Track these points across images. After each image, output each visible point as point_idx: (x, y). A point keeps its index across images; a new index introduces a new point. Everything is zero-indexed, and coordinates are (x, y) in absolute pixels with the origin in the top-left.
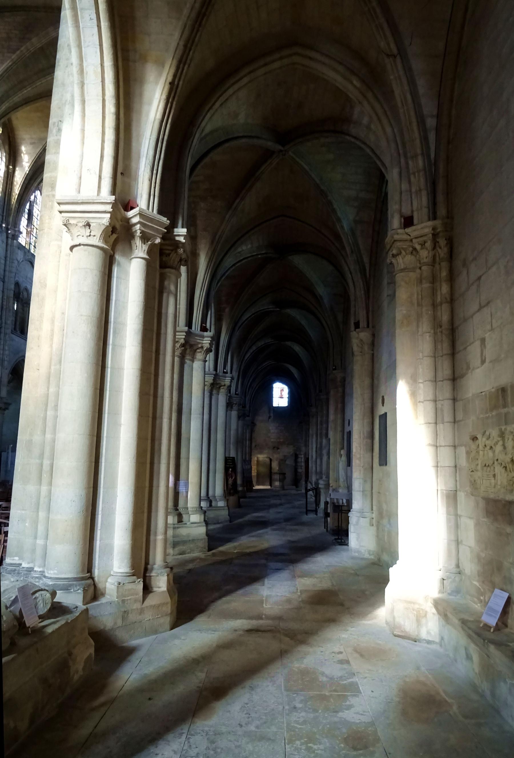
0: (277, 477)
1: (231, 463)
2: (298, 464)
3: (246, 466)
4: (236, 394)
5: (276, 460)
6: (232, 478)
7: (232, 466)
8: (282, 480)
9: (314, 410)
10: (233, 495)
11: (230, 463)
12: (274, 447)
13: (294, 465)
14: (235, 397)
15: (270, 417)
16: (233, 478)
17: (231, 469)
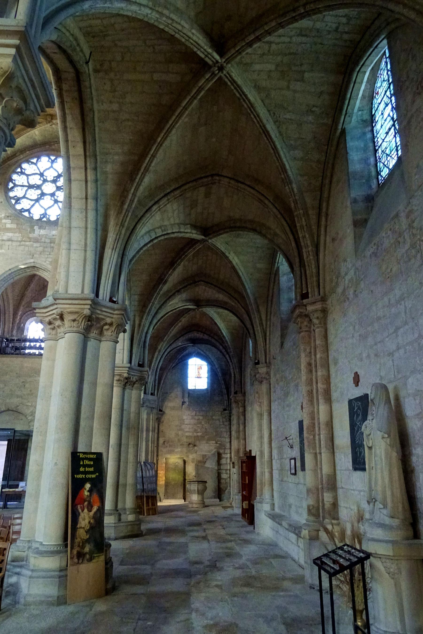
0: (194, 487)
1: (92, 469)
2: (222, 467)
3: (148, 472)
4: (111, 300)
5: (193, 462)
6: (90, 511)
7: (94, 476)
8: (201, 493)
9: (262, 370)
10: (90, 560)
11: (87, 469)
12: (189, 444)
13: (216, 468)
14: (108, 307)
15: (183, 403)
16: (95, 509)
17: (88, 486)
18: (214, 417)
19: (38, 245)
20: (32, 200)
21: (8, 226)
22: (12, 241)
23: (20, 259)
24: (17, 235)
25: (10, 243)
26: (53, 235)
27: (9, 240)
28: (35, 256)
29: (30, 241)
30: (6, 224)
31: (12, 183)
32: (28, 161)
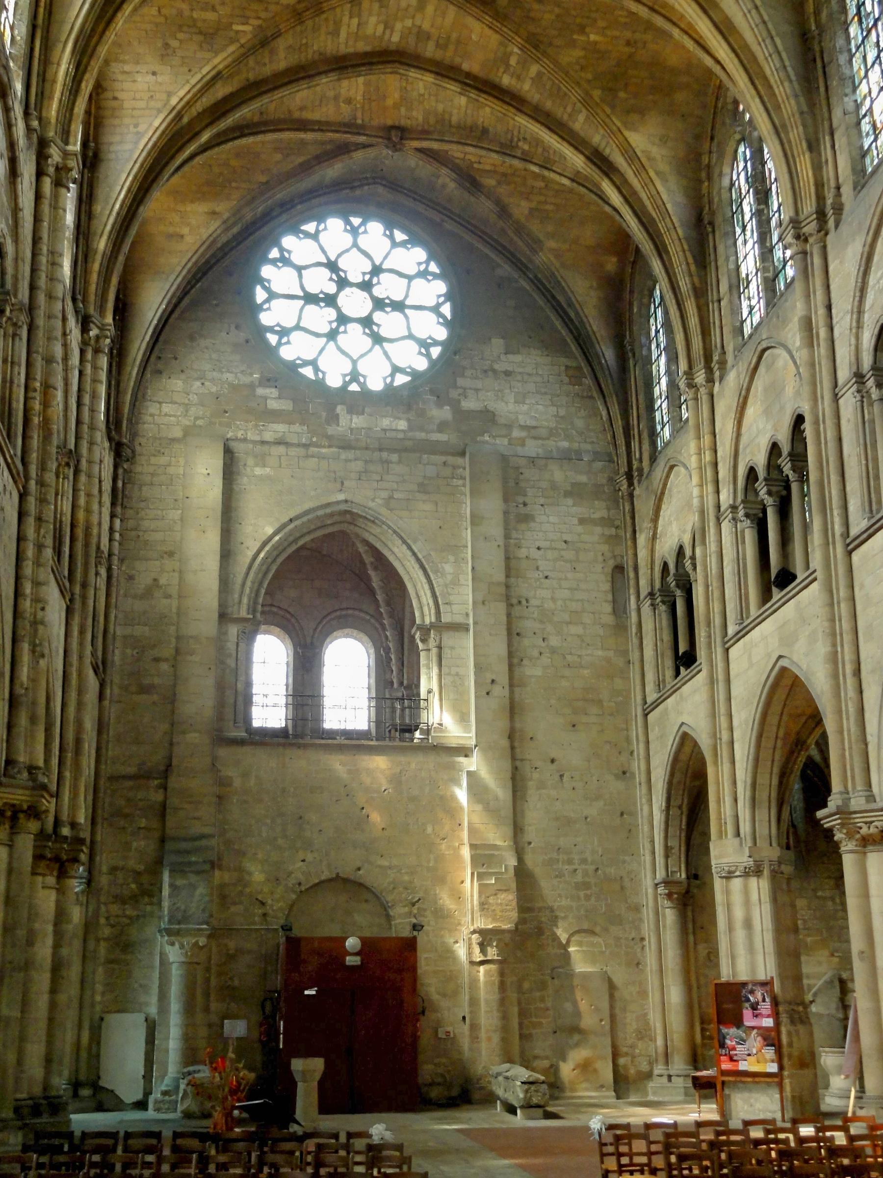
18: (820, 893)
19: (350, 454)
20: (317, 335)
21: (273, 405)
22: (287, 444)
23: (313, 493)
24: (296, 428)
25: (282, 449)
26: (385, 430)
27: (279, 442)
28: (346, 483)
29: (330, 446)
30: (266, 398)
31: (265, 288)
32: (295, 230)
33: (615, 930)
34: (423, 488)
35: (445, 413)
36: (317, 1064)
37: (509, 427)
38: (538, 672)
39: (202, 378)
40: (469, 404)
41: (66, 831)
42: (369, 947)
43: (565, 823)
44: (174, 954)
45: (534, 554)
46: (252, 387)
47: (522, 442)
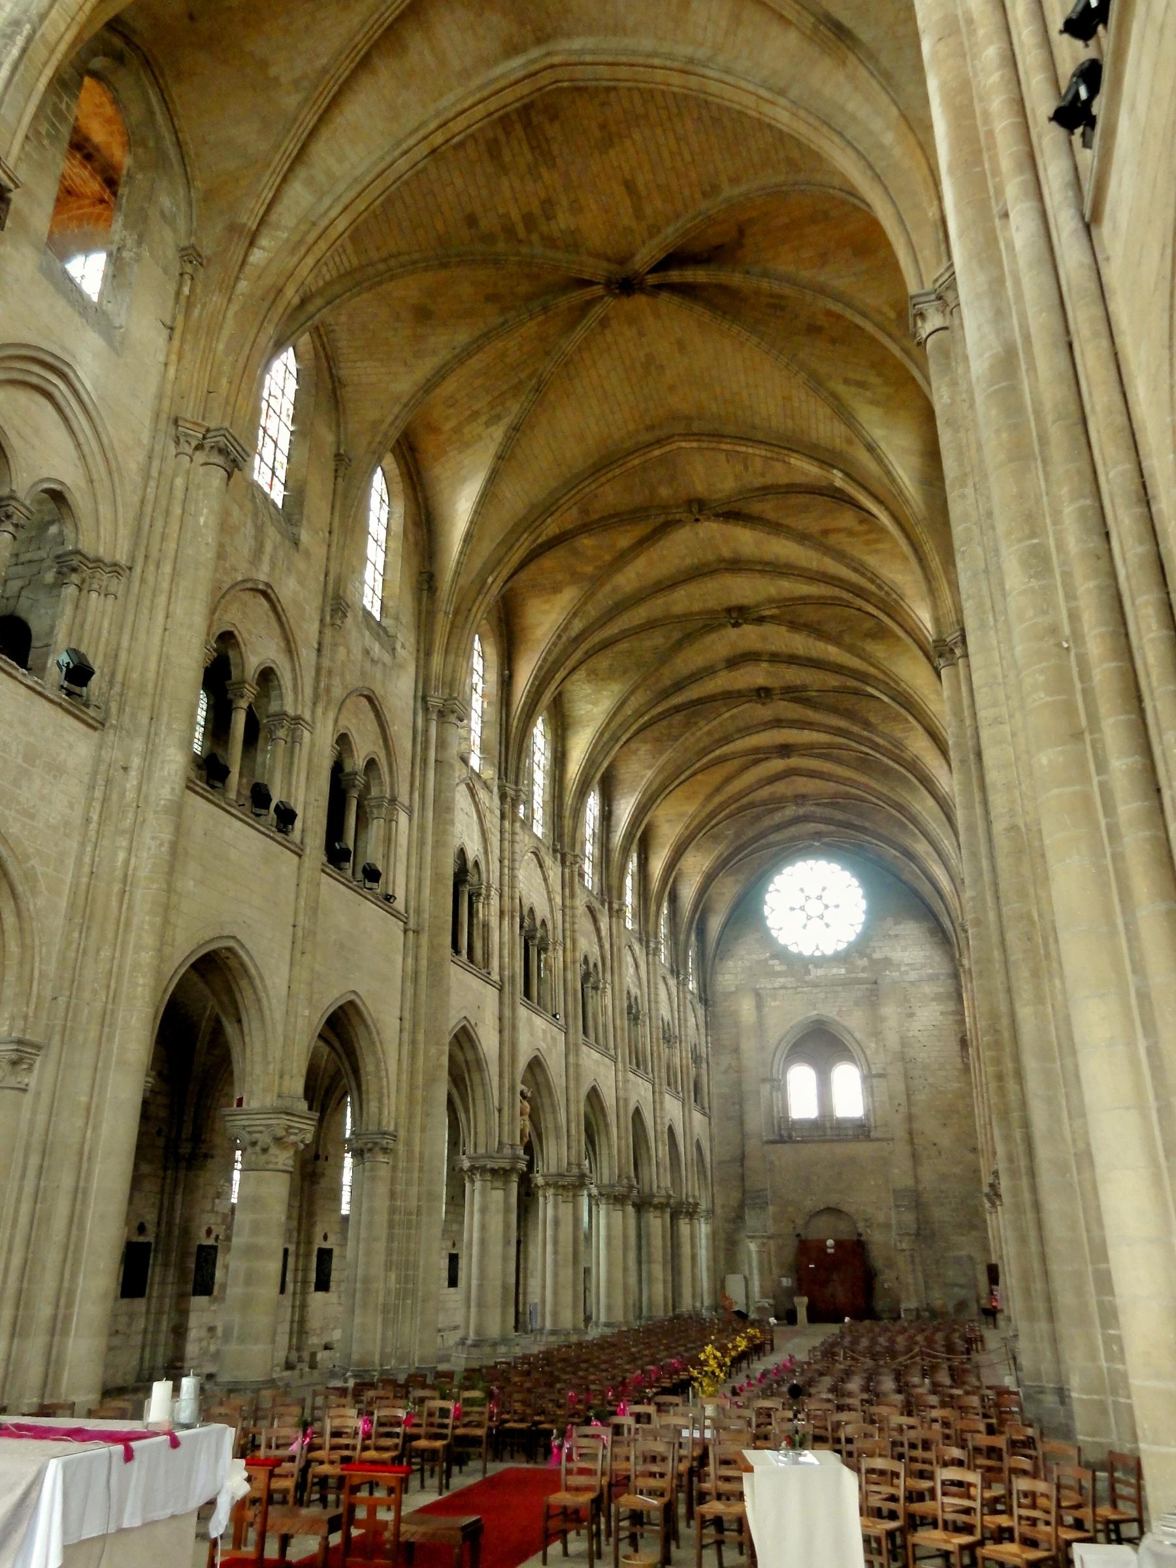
21: (778, 968)
25: (782, 992)
33: (974, 1233)
34: (857, 1004)
35: (864, 962)
36: (805, 1300)
37: (899, 965)
38: (923, 1097)
39: (742, 959)
40: (877, 956)
41: (691, 1200)
42: (839, 1244)
43: (944, 1177)
44: (753, 1247)
45: (917, 1033)
46: (766, 960)
47: (907, 973)
